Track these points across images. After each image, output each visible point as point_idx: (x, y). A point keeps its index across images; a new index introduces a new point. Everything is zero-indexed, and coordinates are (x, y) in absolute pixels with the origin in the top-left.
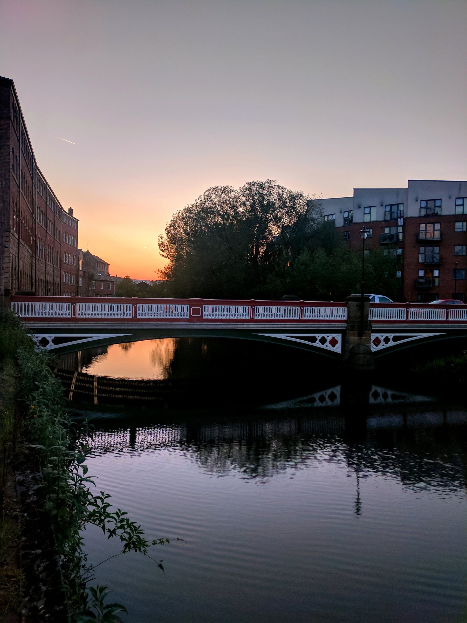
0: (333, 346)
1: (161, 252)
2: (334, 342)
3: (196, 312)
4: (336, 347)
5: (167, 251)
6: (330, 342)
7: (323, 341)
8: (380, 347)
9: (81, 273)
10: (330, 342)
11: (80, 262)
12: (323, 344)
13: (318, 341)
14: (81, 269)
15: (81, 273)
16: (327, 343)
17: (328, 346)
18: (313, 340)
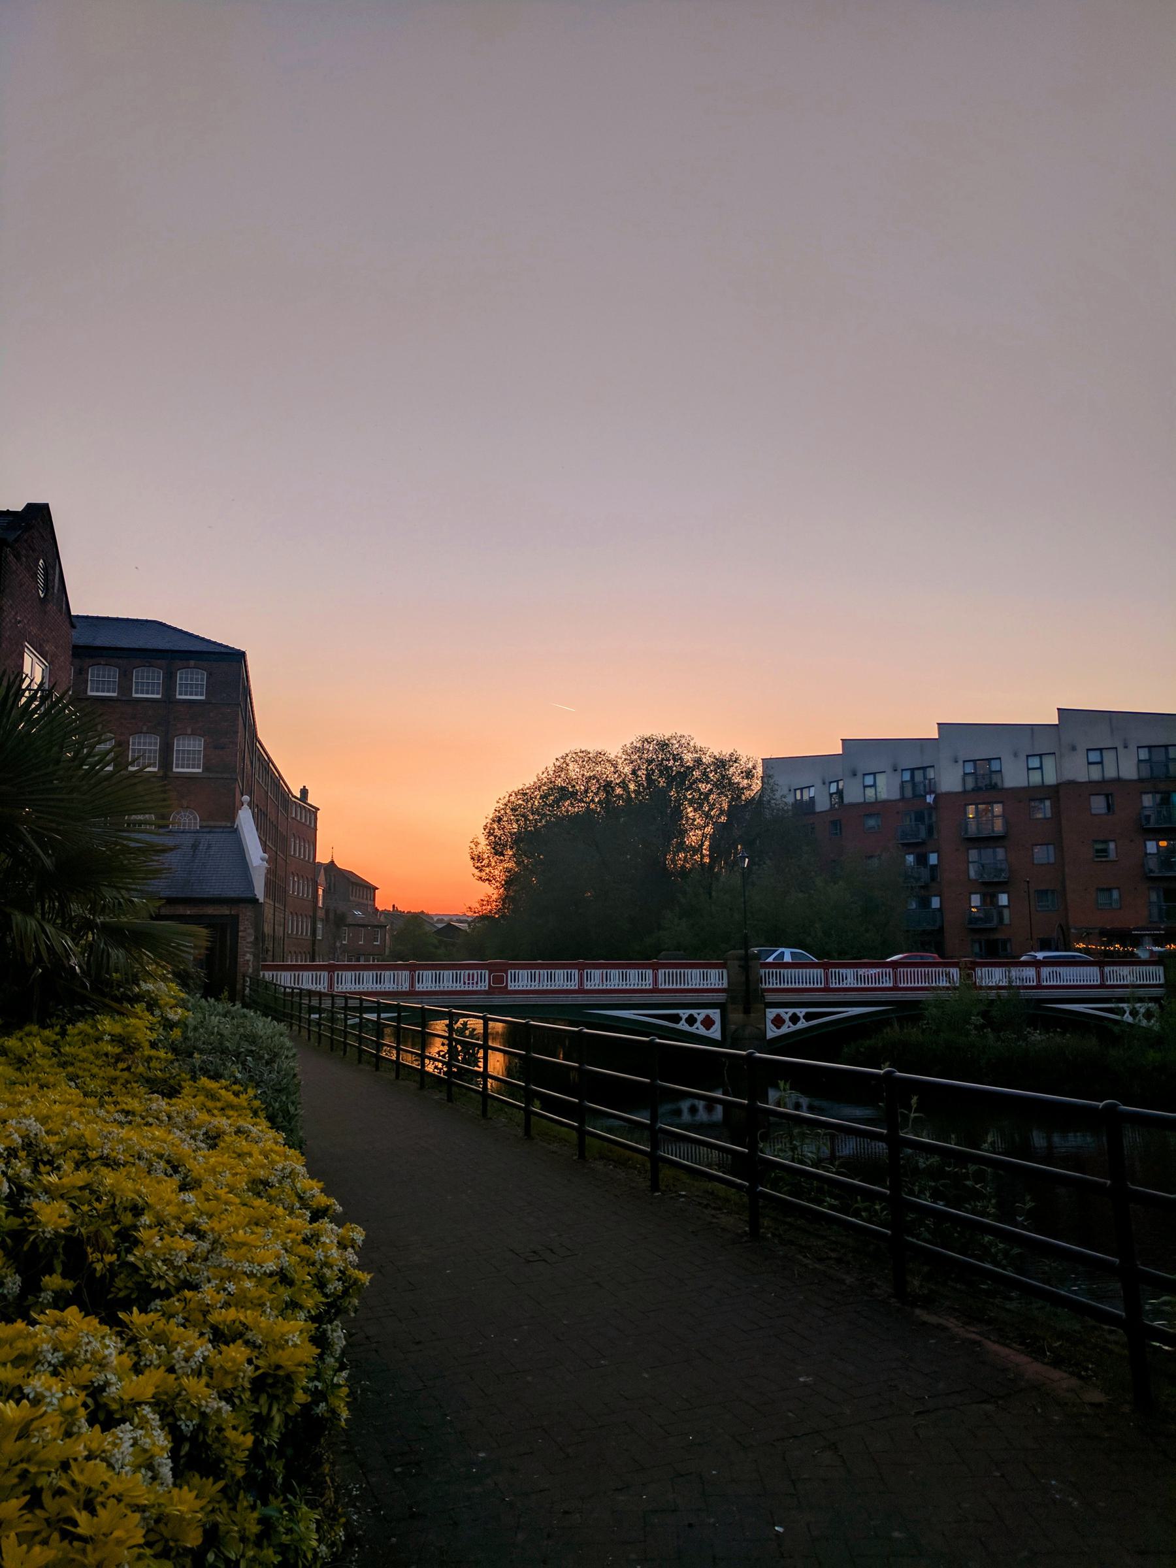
0: (708, 1029)
1: (476, 871)
2: (708, 1022)
3: (498, 980)
4: (712, 1030)
5: (487, 870)
6: (702, 1023)
7: (691, 1020)
8: (784, 1030)
9: (321, 914)
10: (702, 1023)
11: (320, 892)
12: (691, 1025)
13: (683, 1022)
14: (320, 905)
15: (321, 914)
16: (698, 1024)
17: (699, 1029)
18: (676, 1019)
